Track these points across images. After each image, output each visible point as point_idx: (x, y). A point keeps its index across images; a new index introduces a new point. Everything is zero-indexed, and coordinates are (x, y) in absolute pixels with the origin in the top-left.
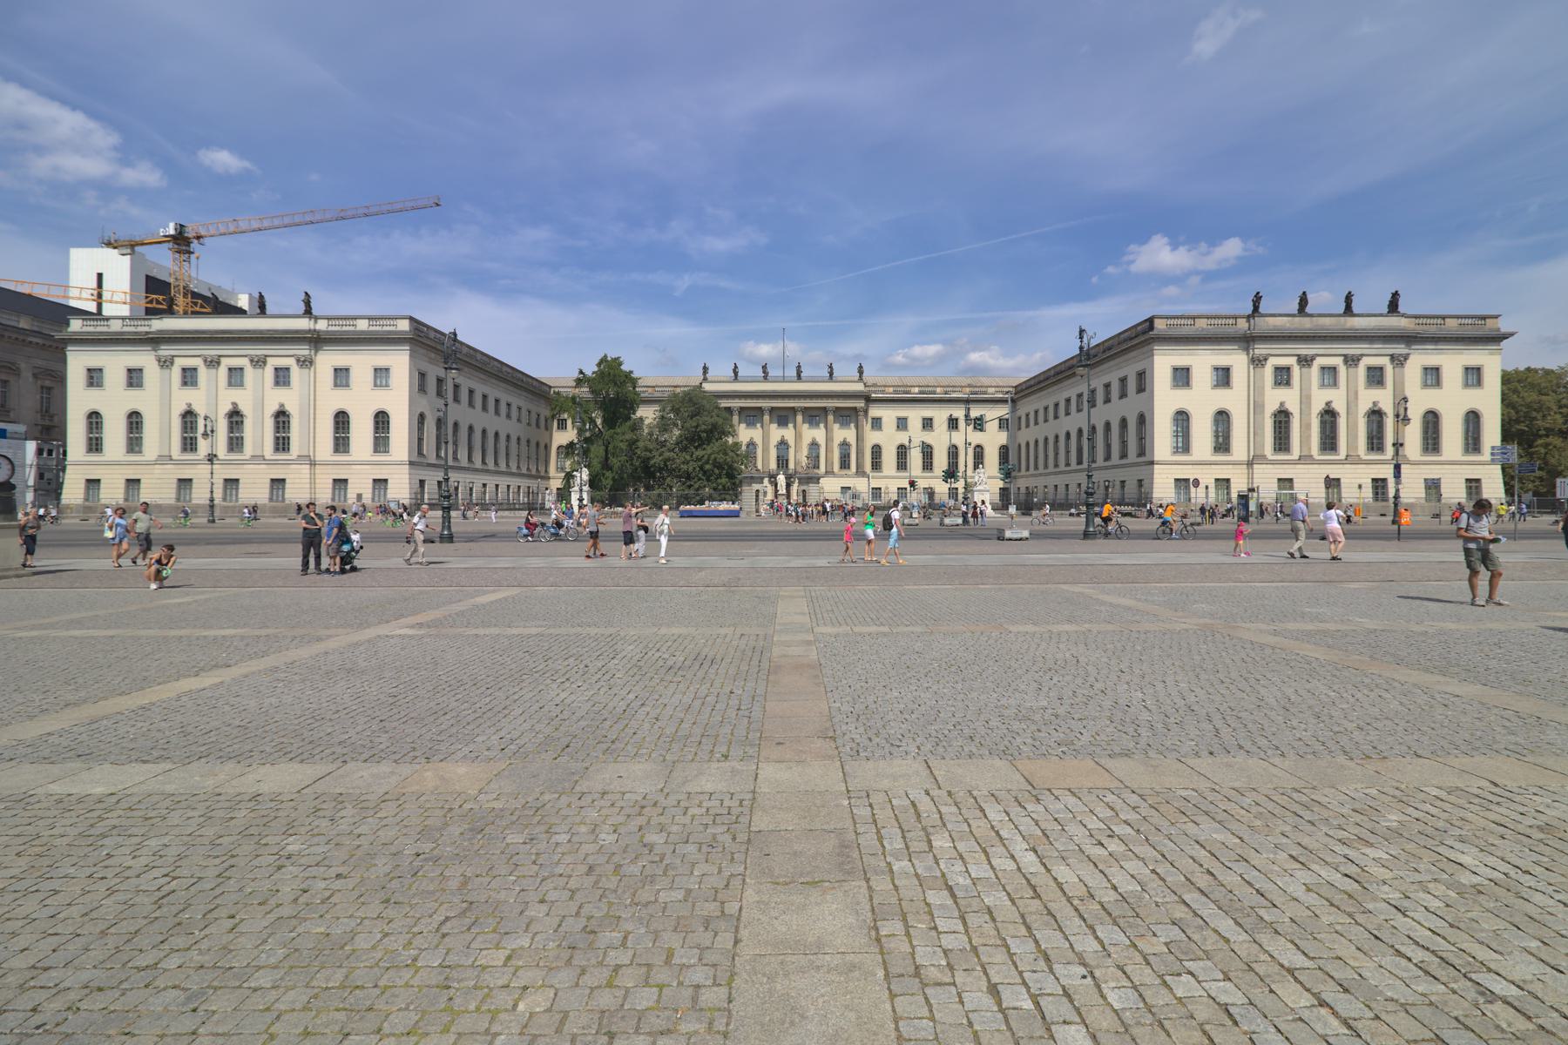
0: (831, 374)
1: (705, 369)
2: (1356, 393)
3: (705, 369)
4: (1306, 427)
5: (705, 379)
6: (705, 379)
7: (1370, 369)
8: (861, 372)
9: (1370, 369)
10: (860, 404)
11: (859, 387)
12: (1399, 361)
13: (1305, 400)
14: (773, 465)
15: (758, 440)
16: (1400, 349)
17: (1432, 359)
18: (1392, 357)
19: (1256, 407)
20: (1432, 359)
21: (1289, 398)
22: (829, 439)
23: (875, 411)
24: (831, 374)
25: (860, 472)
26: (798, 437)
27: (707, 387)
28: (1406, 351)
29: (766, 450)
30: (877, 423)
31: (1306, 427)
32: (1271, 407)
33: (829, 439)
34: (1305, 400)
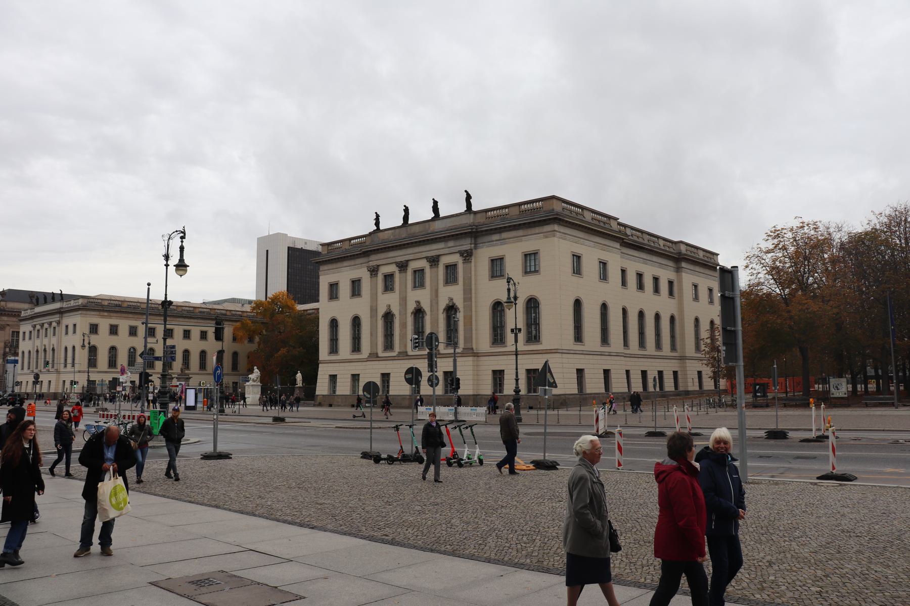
2: (437, 291)
4: (404, 325)
7: (447, 267)
9: (447, 267)
12: (467, 256)
13: (403, 301)
16: (466, 244)
17: (495, 251)
18: (461, 253)
19: (374, 310)
20: (495, 251)
21: (423, 296)
28: (467, 247)
31: (404, 325)
32: (382, 311)
34: (403, 301)
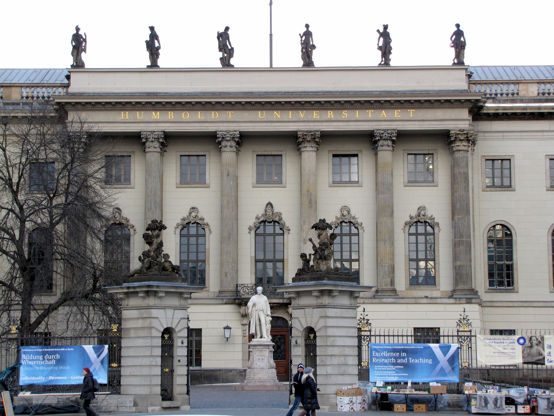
0: (386, 50)
1: (78, 43)
3: (78, 43)
5: (78, 65)
6: (78, 65)
8: (459, 42)
10: (458, 120)
11: (456, 82)
14: (247, 276)
15: (209, 214)
22: (384, 209)
23: (498, 140)
24: (386, 50)
25: (463, 292)
26: (308, 199)
27: (80, 84)
29: (230, 237)
30: (501, 174)
33: (384, 209)
